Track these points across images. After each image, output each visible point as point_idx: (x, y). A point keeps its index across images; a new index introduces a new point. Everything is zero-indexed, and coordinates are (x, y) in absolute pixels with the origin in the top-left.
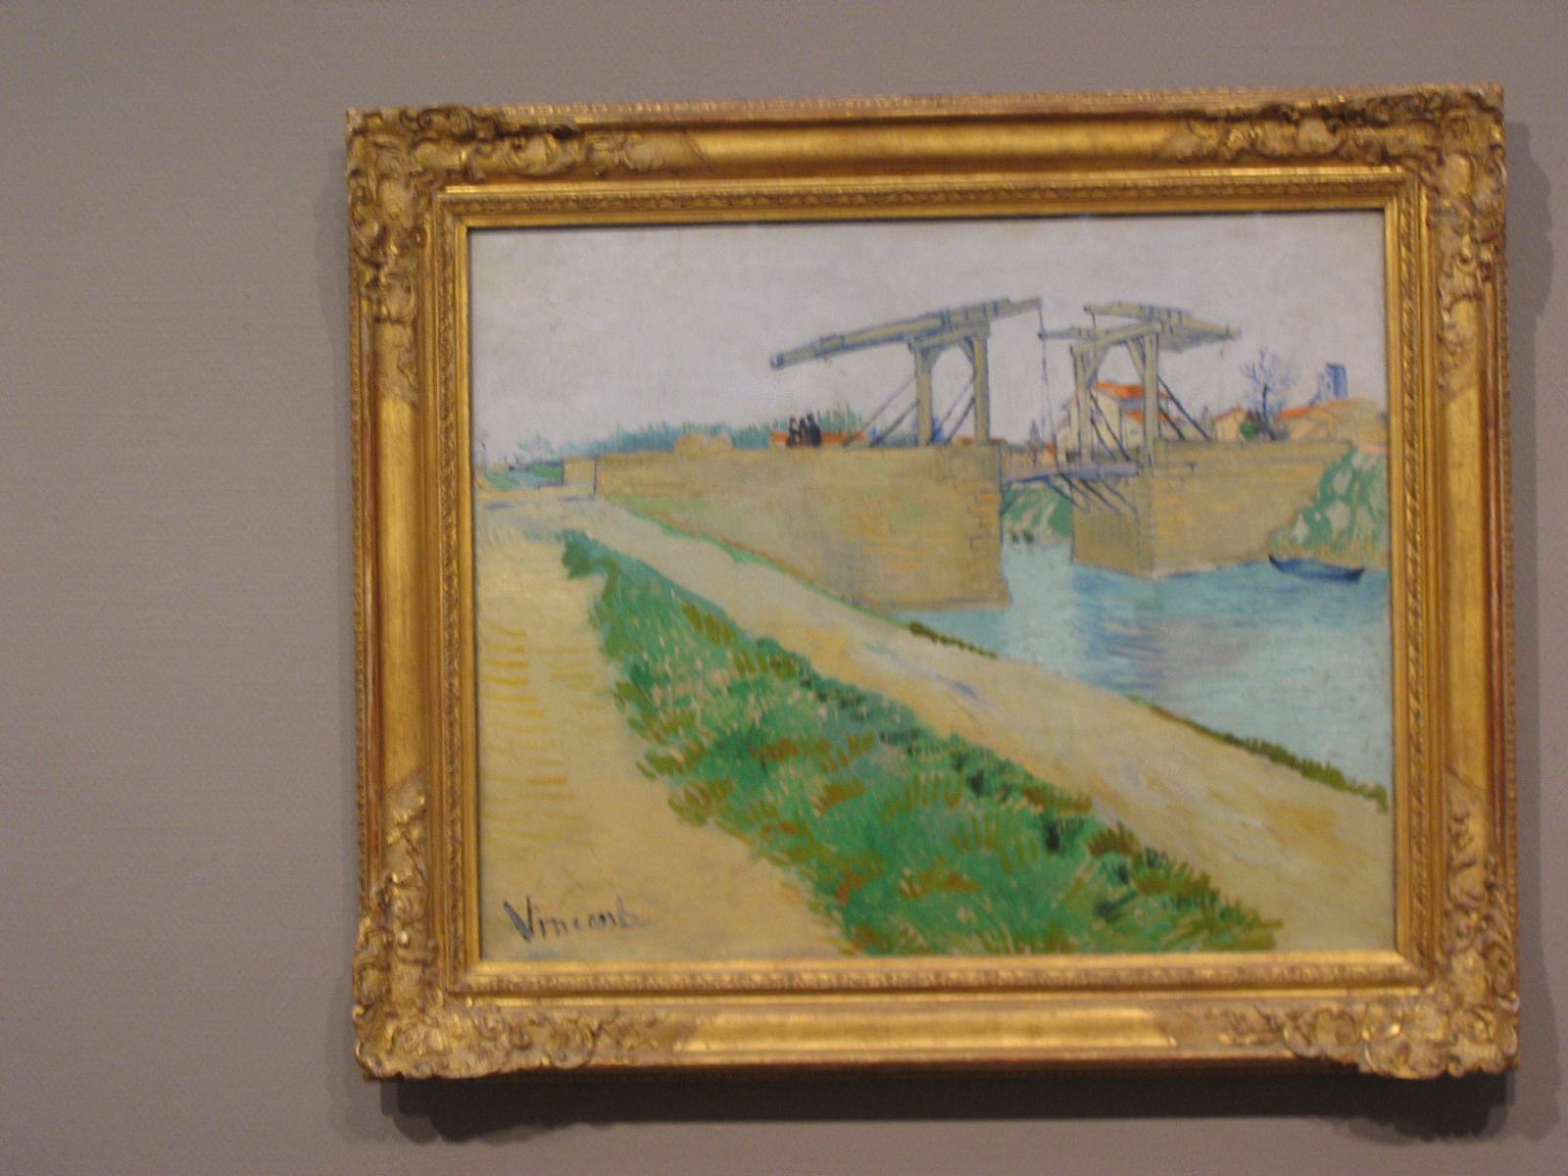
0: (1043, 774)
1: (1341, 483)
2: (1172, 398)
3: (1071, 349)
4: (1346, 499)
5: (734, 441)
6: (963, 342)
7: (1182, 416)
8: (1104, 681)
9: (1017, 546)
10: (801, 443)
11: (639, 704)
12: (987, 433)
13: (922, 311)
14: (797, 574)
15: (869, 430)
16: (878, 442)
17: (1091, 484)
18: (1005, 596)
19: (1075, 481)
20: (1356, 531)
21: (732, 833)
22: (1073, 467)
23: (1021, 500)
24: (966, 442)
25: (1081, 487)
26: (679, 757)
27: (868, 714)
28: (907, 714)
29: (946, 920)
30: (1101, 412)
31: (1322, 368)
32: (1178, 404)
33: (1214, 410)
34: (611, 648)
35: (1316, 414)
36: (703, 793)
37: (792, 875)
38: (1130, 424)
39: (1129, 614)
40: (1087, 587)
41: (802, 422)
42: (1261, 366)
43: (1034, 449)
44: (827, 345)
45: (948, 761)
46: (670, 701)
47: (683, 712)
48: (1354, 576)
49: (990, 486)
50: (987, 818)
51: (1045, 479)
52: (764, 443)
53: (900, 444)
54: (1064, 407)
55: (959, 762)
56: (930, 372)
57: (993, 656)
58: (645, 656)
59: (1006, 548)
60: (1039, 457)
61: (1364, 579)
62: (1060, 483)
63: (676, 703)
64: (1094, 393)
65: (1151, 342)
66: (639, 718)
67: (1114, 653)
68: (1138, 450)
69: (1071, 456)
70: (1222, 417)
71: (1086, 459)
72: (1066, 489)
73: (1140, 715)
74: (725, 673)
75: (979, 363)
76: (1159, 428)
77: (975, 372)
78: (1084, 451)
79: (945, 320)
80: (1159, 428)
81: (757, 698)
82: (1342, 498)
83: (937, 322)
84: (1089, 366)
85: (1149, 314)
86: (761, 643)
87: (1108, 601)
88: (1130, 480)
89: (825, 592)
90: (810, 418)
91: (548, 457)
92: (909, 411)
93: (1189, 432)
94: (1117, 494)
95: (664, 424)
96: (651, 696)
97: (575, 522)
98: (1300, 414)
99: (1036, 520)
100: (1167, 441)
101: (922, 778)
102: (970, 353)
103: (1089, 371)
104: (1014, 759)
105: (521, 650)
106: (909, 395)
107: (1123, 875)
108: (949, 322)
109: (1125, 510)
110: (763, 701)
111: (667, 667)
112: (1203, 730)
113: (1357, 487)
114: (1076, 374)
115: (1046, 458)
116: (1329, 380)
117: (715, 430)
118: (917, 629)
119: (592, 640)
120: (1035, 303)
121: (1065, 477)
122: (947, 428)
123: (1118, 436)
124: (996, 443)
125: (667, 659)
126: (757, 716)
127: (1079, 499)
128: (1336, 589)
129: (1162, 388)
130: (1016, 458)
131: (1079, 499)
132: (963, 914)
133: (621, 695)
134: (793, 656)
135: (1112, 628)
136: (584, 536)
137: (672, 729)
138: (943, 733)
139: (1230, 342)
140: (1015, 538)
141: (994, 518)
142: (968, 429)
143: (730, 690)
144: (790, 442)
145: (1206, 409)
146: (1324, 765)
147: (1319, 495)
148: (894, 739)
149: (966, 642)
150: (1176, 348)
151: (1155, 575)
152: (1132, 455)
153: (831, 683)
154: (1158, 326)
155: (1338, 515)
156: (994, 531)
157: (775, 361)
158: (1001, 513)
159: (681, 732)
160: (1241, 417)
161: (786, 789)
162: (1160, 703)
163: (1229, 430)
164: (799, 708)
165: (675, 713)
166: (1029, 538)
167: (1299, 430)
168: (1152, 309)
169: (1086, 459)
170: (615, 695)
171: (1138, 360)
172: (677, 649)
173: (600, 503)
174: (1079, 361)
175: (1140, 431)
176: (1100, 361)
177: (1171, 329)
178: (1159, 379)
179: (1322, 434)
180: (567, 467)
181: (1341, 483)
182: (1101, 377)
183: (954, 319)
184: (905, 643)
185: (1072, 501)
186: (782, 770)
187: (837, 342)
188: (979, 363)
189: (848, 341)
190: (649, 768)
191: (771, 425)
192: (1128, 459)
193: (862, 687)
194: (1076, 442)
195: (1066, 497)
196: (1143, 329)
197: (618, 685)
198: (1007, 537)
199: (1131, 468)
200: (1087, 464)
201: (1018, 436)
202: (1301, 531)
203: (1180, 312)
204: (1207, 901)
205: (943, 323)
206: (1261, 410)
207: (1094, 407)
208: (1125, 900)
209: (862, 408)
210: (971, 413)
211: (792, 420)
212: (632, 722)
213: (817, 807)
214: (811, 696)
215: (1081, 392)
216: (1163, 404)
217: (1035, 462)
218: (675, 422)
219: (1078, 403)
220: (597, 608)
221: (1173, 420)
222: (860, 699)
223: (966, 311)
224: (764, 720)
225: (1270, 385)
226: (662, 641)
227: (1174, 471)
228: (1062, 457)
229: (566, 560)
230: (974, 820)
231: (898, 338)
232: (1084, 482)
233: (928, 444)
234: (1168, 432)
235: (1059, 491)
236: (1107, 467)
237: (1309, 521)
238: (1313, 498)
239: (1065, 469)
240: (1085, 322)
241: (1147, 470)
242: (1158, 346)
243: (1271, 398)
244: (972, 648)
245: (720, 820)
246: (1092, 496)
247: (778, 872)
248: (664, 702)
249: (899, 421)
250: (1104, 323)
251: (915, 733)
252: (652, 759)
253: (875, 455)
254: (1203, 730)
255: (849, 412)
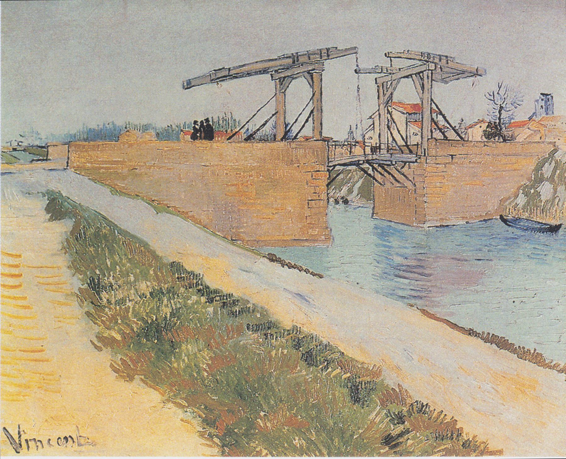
0: (350, 352)
1: (547, 170)
2: (441, 113)
3: (376, 79)
4: (551, 180)
5: (158, 134)
6: (306, 74)
7: (448, 126)
8: (392, 294)
9: (337, 206)
10: (201, 138)
11: (92, 303)
12: (321, 133)
13: (280, 54)
14: (197, 221)
15: (243, 131)
16: (250, 138)
17: (386, 166)
18: (329, 238)
19: (376, 166)
20: (557, 200)
21: (151, 387)
22: (375, 157)
23: (341, 176)
24: (307, 139)
25: (380, 169)
26: (118, 337)
27: (239, 311)
28: (264, 313)
29: (286, 445)
30: (394, 122)
31: (538, 96)
32: (444, 117)
33: (468, 122)
34: (75, 267)
35: (533, 126)
36: (131, 360)
37: (189, 416)
38: (413, 128)
39: (408, 251)
40: (383, 234)
41: (202, 122)
42: (498, 93)
43: (351, 145)
44: (220, 75)
45: (290, 343)
46: (113, 301)
47: (120, 308)
48: (554, 229)
49: (322, 168)
50: (315, 379)
51: (357, 164)
52: (178, 139)
53: (263, 140)
54: (370, 117)
55: (297, 345)
56: (284, 92)
57: (321, 277)
58: (98, 272)
59: (330, 207)
60: (353, 150)
61: (561, 232)
62: (366, 166)
63: (118, 303)
64: (389, 108)
65: (428, 77)
66: (92, 311)
67: (400, 277)
68: (418, 145)
69: (374, 149)
70: (471, 127)
71: (384, 152)
72: (370, 171)
73: (415, 316)
74: (149, 283)
75: (317, 89)
76: (432, 132)
77: (314, 95)
78: (383, 146)
79: (295, 59)
80: (432, 132)
81: (169, 299)
82: (547, 180)
83: (290, 61)
84: (387, 91)
85: (426, 58)
86: (172, 264)
87: (395, 242)
88: (411, 164)
89: (214, 234)
90: (207, 120)
91: (37, 143)
92: (271, 118)
93: (451, 135)
94: (403, 174)
95: (113, 123)
96: (101, 299)
97: (54, 186)
98: (522, 124)
99: (350, 191)
100: (436, 140)
101: (273, 353)
102: (311, 84)
103: (388, 94)
104: (331, 343)
105: (17, 266)
106: (271, 109)
107: (400, 419)
108: (298, 61)
109: (408, 184)
110: (172, 301)
111: (111, 278)
112: (454, 326)
113: (558, 172)
114: (378, 98)
115: (358, 150)
116: (543, 103)
117: (145, 128)
118: (272, 258)
119: (62, 261)
120: (353, 50)
121: (368, 162)
122: (295, 130)
123: (405, 138)
124: (326, 140)
125: (111, 273)
126: (168, 311)
127: (378, 177)
128: (543, 237)
129: (434, 106)
130: (339, 149)
131: (378, 177)
132: (296, 442)
133: (82, 296)
134: (192, 273)
135: (398, 260)
136: (59, 192)
137: (113, 319)
138: (287, 324)
139: (478, 77)
140: (337, 202)
141: (324, 187)
142: (308, 131)
143: (151, 294)
144: (194, 137)
145: (463, 120)
146: (532, 351)
147: (533, 176)
148: (257, 328)
149: (304, 268)
150: (444, 81)
151: (426, 226)
152: (414, 149)
153: (216, 291)
154: (432, 66)
155: (546, 190)
156: (324, 196)
157: (185, 84)
158: (327, 185)
159: (119, 321)
160: (484, 126)
161: (186, 361)
162: (425, 308)
163: (477, 134)
164: (196, 306)
165: (115, 308)
166: (346, 202)
167: (522, 135)
168: (429, 54)
169: (384, 152)
170: (77, 296)
171: (419, 87)
172: (117, 267)
173: (71, 171)
174: (381, 88)
175: (420, 134)
176: (394, 89)
177: (441, 68)
178: (432, 100)
179: (537, 139)
180: (50, 150)
181: (547, 170)
182: (395, 99)
183: (301, 60)
184: (264, 265)
185: (374, 178)
186: (184, 347)
187: (226, 73)
188: (317, 89)
189: (232, 72)
190: (99, 344)
191: (182, 126)
192: (411, 152)
193: (237, 294)
194: (378, 142)
195: (370, 175)
196: (423, 68)
197: (80, 289)
198: (331, 200)
199: (413, 158)
200: (384, 155)
201: (341, 136)
202: (521, 200)
203: (447, 57)
204: (455, 436)
205: (294, 62)
206: (498, 121)
207: (389, 118)
208: (401, 435)
209: (241, 116)
210: (311, 119)
211: (195, 122)
212: (88, 314)
213: (205, 370)
214: (203, 299)
215: (382, 106)
216: (434, 115)
217: (350, 152)
218: (120, 122)
219: (379, 114)
220: (67, 240)
221: (440, 127)
222: (235, 302)
223: (309, 55)
224: (172, 314)
225: (504, 105)
226: (109, 263)
227: (439, 160)
228: (368, 150)
229: (48, 209)
230: (306, 381)
231: (264, 71)
232: (380, 165)
233: (282, 140)
234: (438, 135)
235: (366, 172)
236: (398, 156)
237: (526, 194)
238: (529, 179)
239: (370, 157)
240: (385, 62)
241: (423, 159)
242: (432, 80)
243: (504, 114)
244: (307, 271)
245: (143, 377)
246: (386, 174)
247: (180, 411)
248: (109, 301)
249: (264, 125)
250: (397, 63)
251: (271, 325)
252: (100, 337)
253: (248, 144)
254: (454, 326)
255: (232, 117)
